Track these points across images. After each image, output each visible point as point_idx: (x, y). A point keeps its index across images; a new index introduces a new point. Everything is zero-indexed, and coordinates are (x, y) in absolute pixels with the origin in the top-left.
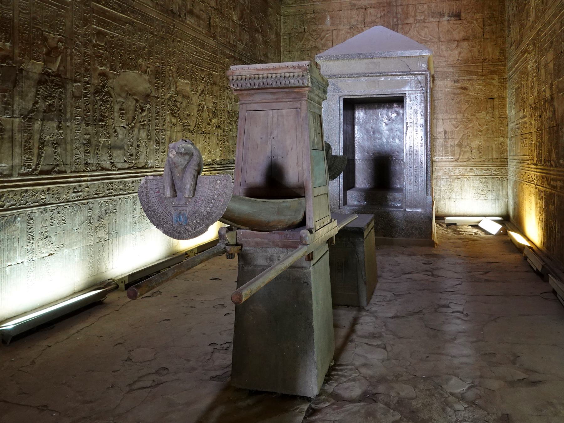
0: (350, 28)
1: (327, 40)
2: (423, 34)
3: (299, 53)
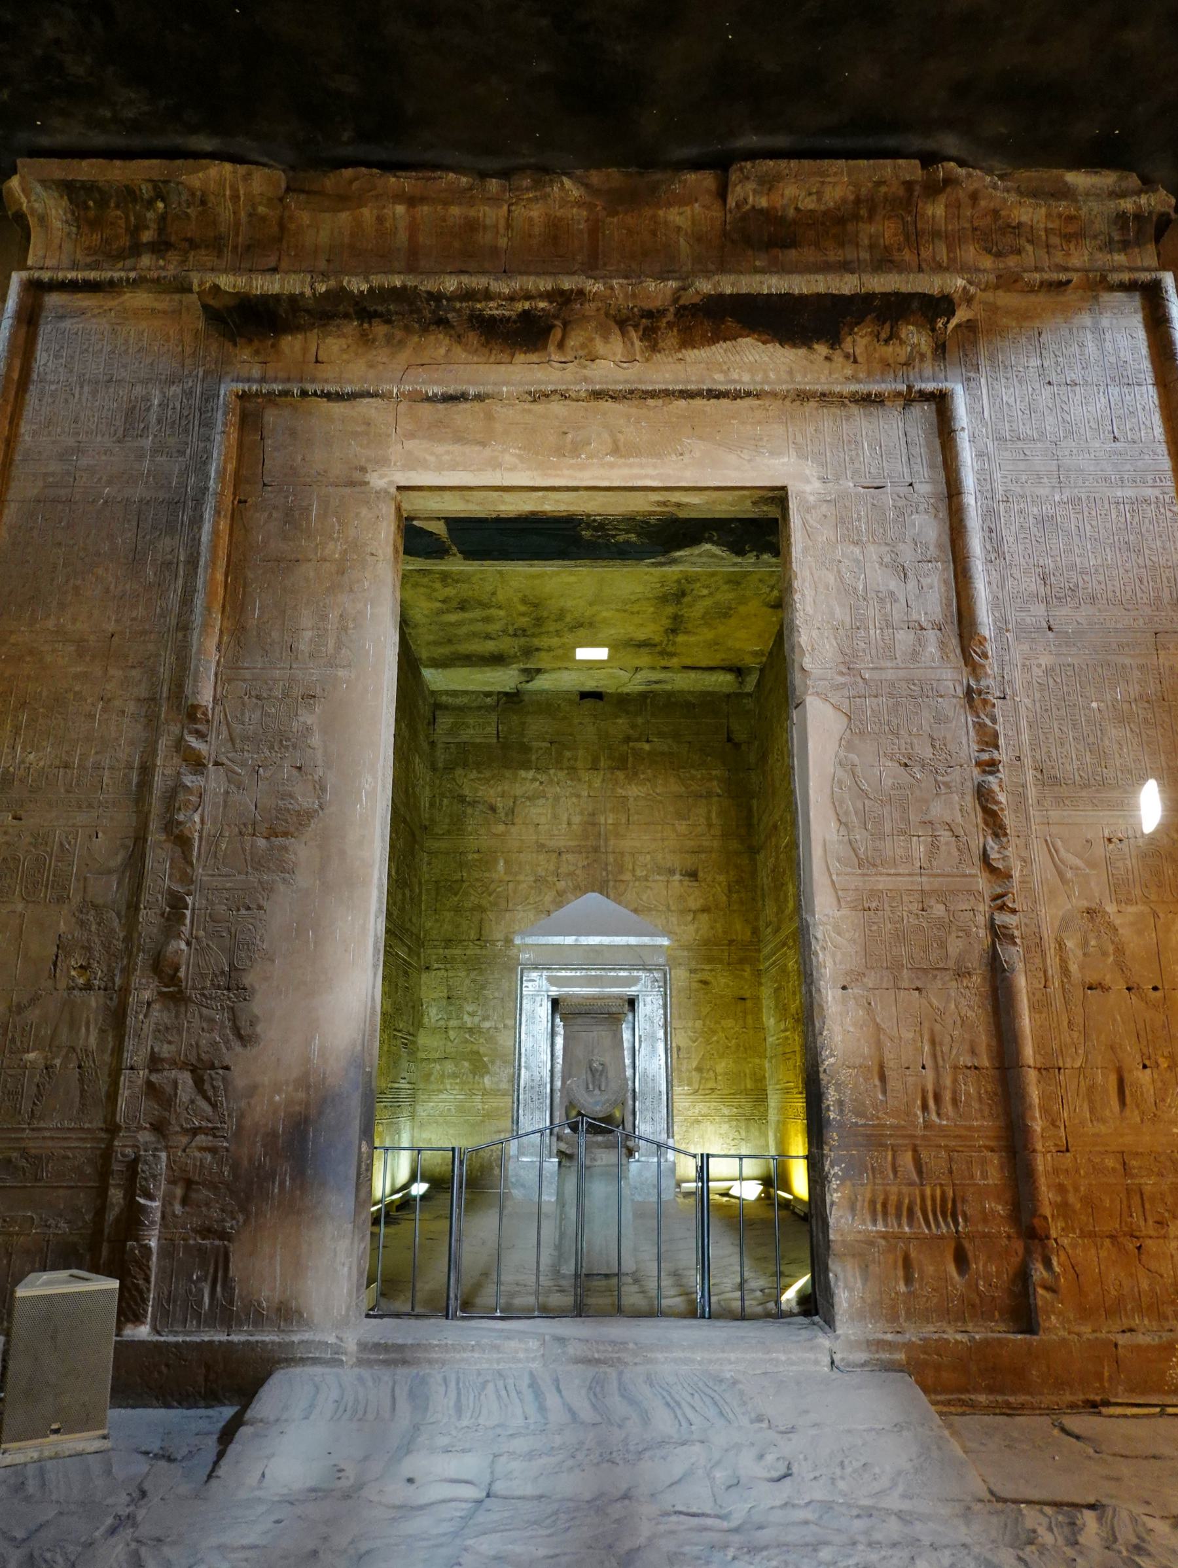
2: (644, 898)
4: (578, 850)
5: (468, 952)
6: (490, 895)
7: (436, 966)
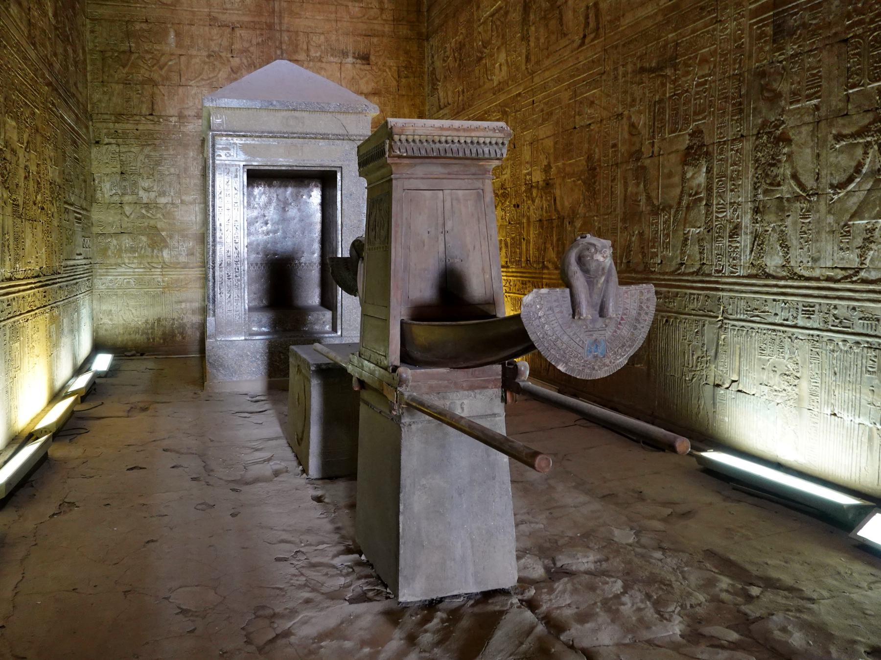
0: (209, 56)
1: (170, 70)
3: (121, 86)
4: (252, 26)
5: (141, 127)
6: (161, 69)
7: (107, 140)
